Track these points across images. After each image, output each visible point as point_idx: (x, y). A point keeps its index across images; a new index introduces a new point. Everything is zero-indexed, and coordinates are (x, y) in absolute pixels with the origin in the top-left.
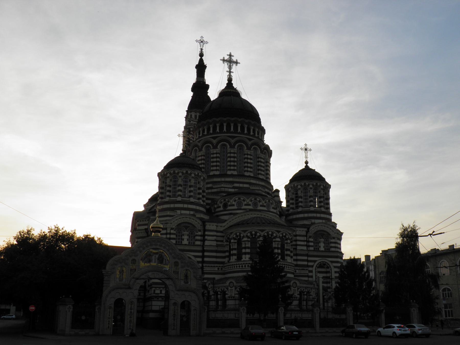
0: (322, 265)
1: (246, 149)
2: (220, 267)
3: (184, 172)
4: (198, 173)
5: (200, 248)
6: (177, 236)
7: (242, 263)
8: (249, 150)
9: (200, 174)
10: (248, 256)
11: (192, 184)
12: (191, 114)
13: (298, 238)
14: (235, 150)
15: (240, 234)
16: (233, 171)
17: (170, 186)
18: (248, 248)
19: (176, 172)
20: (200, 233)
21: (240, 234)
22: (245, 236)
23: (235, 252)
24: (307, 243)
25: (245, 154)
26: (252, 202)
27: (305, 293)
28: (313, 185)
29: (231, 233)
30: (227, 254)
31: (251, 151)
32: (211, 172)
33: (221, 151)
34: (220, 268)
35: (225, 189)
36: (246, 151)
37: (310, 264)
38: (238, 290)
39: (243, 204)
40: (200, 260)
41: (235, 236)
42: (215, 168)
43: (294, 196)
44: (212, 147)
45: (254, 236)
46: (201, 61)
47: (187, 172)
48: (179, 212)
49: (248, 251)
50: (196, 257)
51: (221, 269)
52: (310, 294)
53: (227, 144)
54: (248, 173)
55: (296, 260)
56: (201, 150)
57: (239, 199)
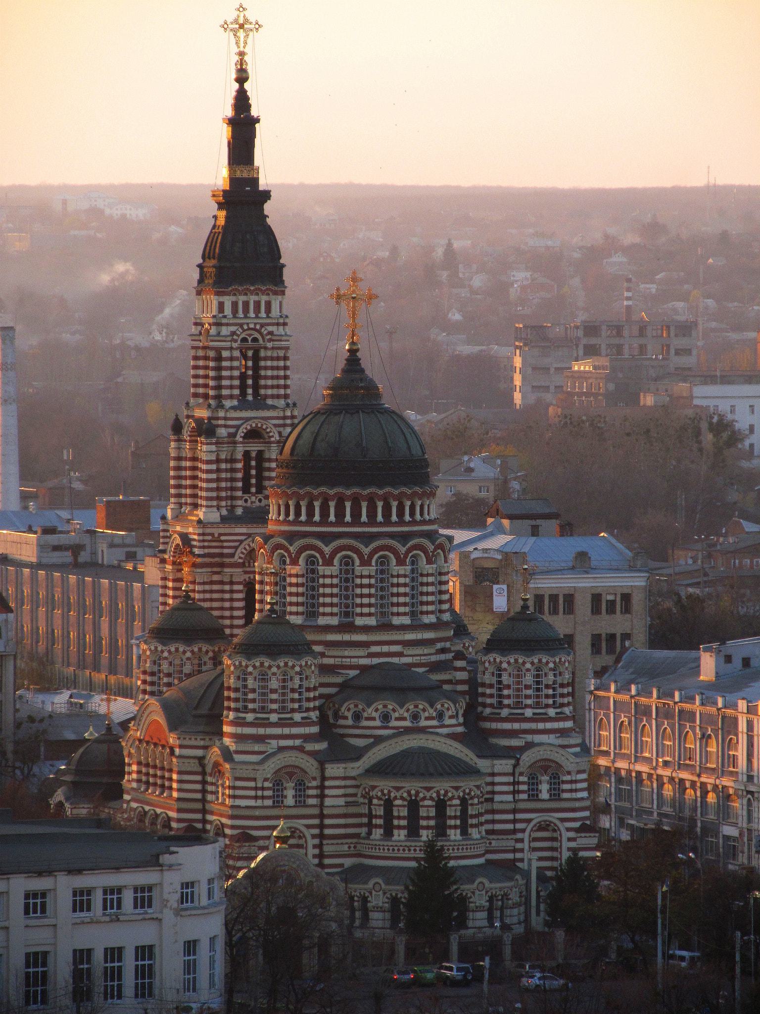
0: (543, 827)
1: (394, 563)
2: (351, 843)
3: (282, 664)
4: (306, 662)
5: (316, 811)
6: (274, 792)
7: (394, 844)
8: (401, 565)
9: (309, 663)
10: (404, 832)
11: (297, 686)
12: (221, 299)
13: (497, 779)
14: (372, 569)
15: (389, 792)
16: (368, 618)
17: (253, 691)
18: (404, 818)
19: (266, 664)
20: (314, 783)
21: (389, 792)
22: (398, 797)
23: (380, 822)
24: (514, 788)
25: (392, 576)
26: (410, 712)
27: (500, 897)
28: (532, 663)
29: (374, 788)
30: (365, 820)
31: (407, 567)
32: (321, 618)
33: (341, 570)
34: (352, 846)
35: (353, 660)
36: (396, 569)
37: (519, 826)
38: (389, 896)
40: (316, 831)
41: (379, 794)
42: (328, 610)
43: (494, 680)
44: (320, 561)
45: (413, 798)
46: (242, 101)
47: (286, 664)
48: (274, 743)
49: (404, 823)
50: (308, 827)
51: (355, 847)
52: (510, 896)
53: (355, 556)
54: (400, 618)
55: (493, 822)
56: (295, 562)
57: (385, 706)
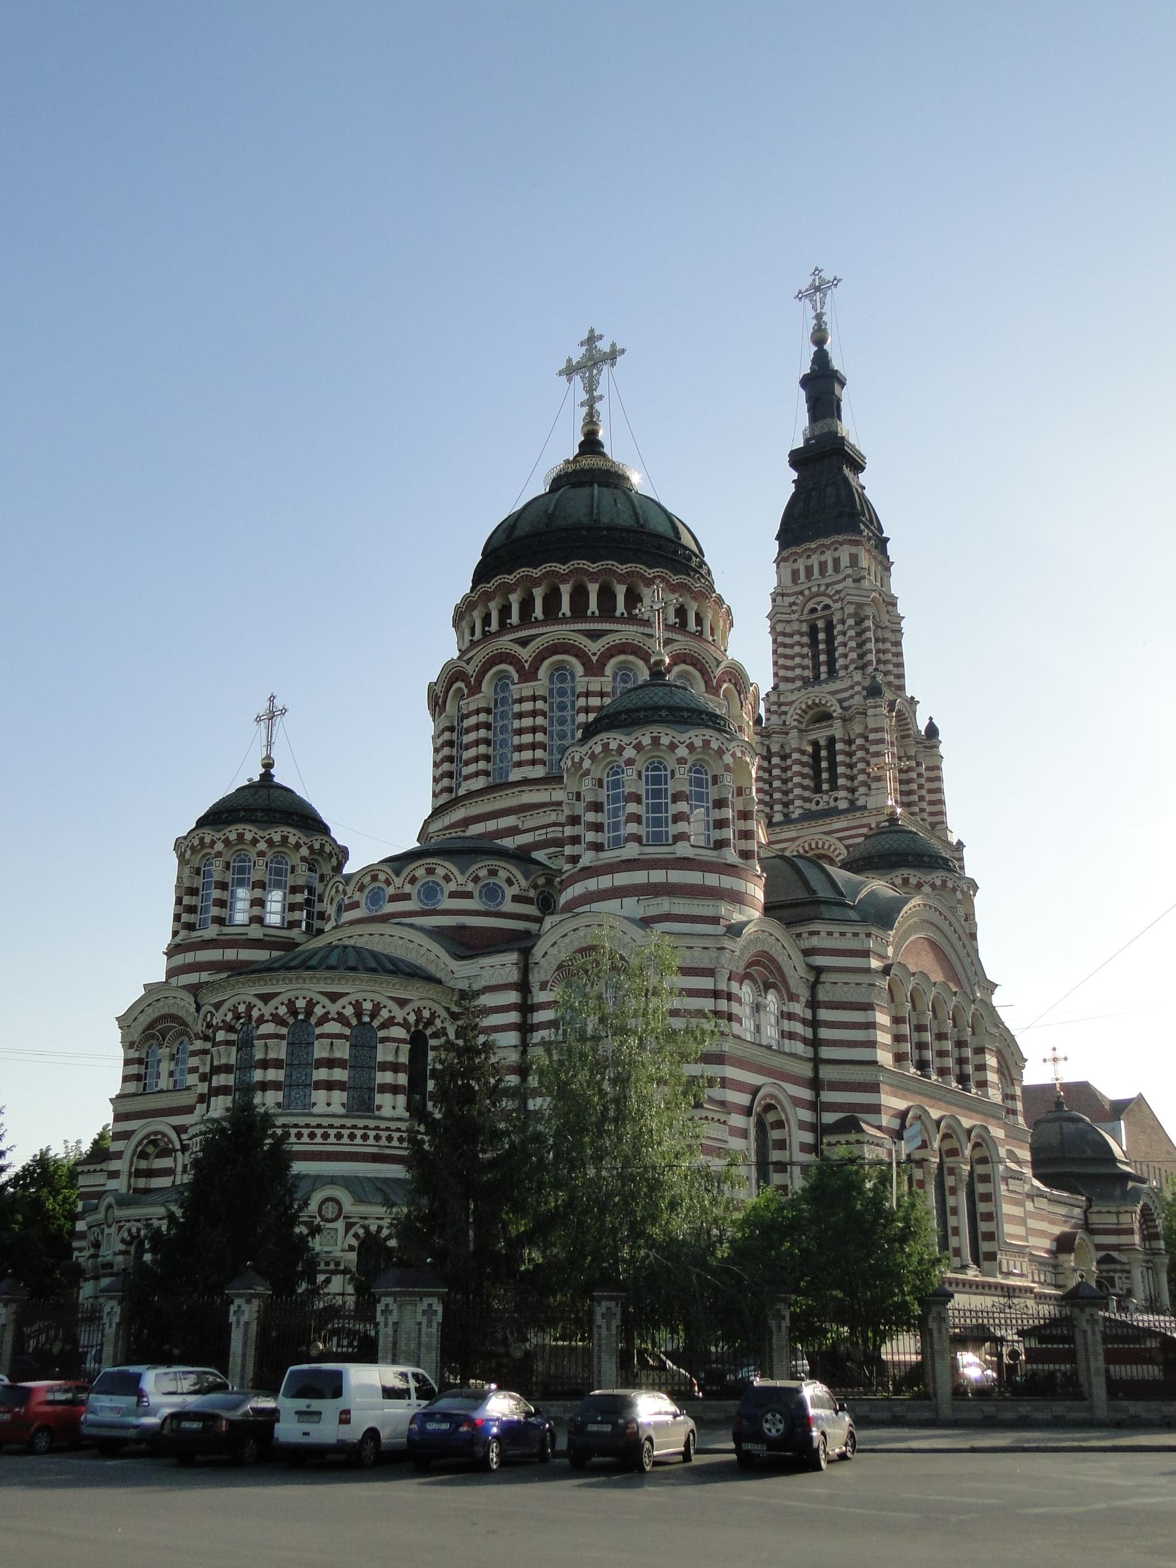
25: (579, 696)
31: (602, 679)
36: (582, 682)
39: (443, 893)
46: (821, 359)
